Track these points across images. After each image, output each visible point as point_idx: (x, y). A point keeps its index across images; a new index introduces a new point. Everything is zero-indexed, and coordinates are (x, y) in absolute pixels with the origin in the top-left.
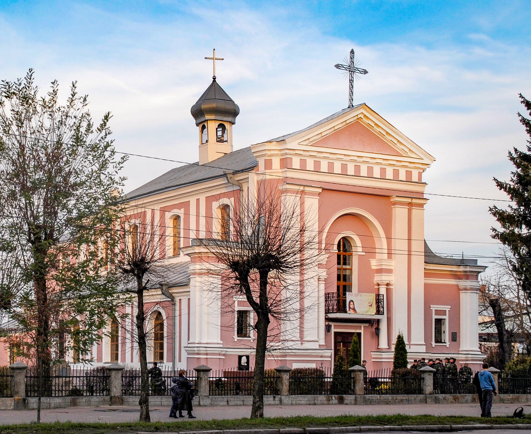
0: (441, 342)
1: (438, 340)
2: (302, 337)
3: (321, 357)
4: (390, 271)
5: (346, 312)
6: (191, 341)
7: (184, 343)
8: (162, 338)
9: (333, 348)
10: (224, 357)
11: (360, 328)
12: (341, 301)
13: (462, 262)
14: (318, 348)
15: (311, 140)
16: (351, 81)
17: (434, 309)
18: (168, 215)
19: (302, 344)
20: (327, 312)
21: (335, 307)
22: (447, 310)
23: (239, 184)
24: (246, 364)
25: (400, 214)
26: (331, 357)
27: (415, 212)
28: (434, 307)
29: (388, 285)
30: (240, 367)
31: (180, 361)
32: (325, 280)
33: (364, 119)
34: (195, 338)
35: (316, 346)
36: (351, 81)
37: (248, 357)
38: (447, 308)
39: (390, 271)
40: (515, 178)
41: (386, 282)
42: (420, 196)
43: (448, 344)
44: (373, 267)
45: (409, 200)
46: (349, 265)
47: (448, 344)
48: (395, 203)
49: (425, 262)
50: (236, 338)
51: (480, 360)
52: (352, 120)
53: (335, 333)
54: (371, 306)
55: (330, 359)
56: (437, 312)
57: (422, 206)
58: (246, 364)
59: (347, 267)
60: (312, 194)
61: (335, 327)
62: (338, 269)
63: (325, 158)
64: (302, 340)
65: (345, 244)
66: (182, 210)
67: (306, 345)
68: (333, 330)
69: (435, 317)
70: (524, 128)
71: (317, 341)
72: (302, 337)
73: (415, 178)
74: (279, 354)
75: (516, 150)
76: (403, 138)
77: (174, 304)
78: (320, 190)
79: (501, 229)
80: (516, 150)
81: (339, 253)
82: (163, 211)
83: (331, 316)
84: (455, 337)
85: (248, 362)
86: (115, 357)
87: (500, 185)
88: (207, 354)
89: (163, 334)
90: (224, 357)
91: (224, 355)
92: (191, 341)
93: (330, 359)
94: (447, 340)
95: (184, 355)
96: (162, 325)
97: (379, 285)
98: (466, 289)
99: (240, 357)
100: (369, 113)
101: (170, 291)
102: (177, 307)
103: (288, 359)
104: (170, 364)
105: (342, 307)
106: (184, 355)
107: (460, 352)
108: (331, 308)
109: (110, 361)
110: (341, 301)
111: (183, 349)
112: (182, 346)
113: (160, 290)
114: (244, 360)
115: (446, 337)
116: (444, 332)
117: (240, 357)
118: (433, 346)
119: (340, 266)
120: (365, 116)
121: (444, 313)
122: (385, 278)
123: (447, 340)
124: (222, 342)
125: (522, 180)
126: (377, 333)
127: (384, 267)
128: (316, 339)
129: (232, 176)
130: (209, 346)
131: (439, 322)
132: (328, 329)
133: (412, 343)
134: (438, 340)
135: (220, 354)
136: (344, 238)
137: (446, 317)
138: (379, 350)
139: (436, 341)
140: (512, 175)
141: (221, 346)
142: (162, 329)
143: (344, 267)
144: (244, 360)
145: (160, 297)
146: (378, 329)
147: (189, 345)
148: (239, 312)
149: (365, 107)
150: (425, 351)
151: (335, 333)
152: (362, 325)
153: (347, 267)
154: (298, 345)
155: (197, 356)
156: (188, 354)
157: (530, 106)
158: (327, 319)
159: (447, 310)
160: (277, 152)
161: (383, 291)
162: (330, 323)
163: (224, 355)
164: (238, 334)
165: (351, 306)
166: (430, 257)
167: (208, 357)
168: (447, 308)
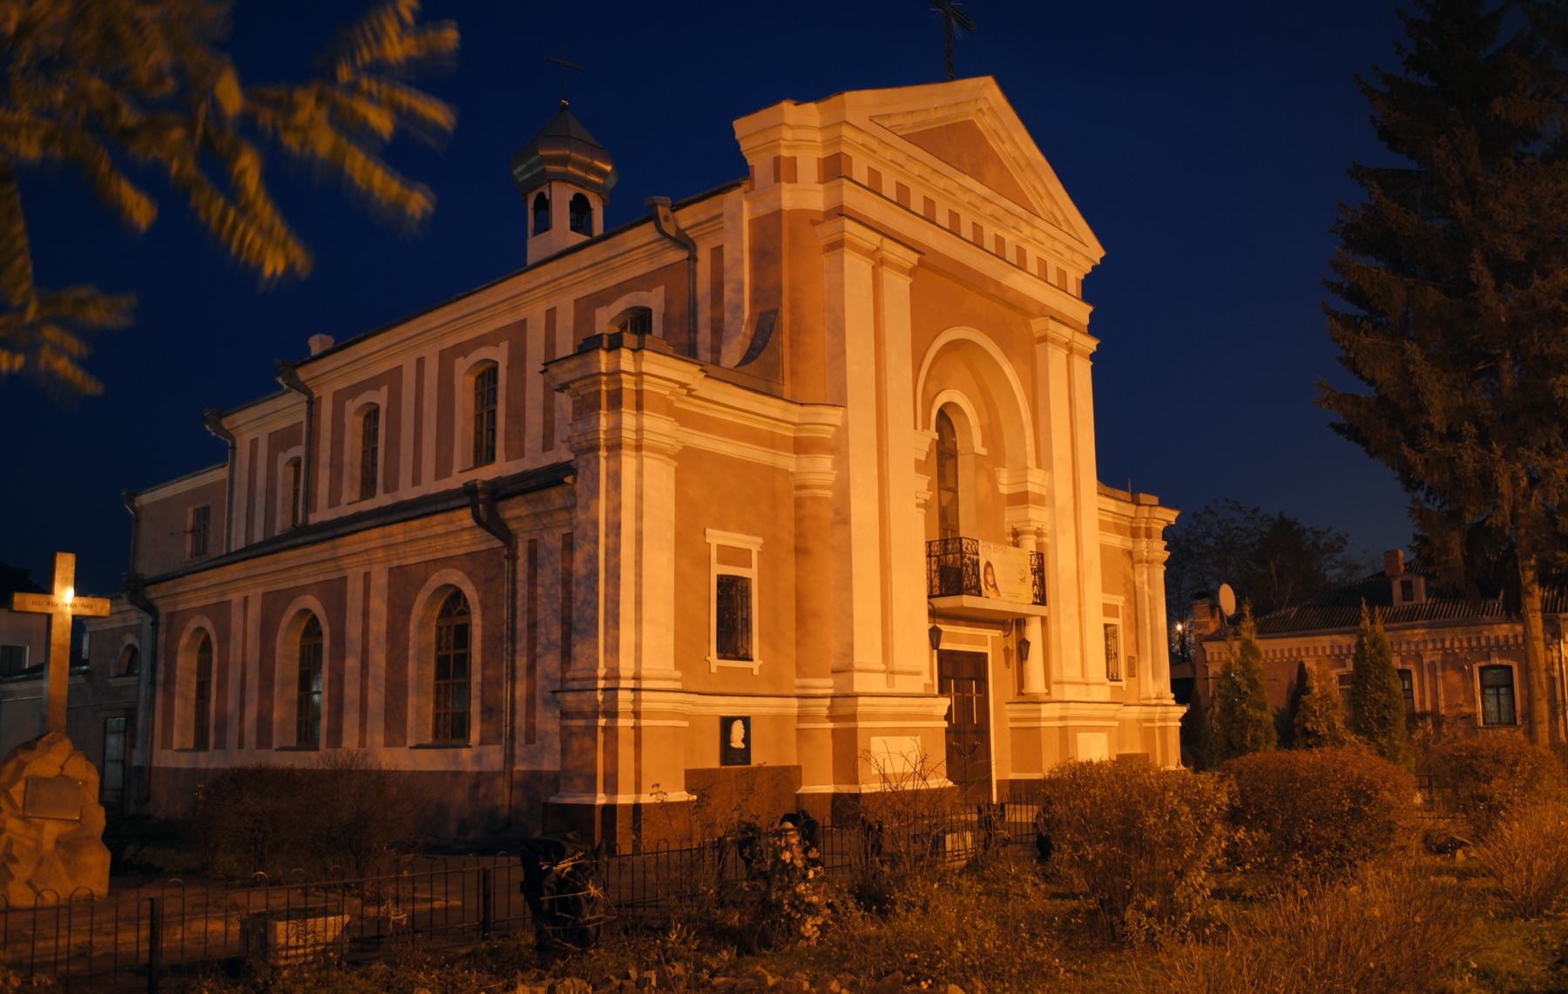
5: (979, 594)
10: (686, 724)
11: (981, 640)
14: (921, 691)
19: (889, 683)
30: (729, 754)
37: (746, 721)
54: (1023, 580)
60: (898, 268)
67: (904, 684)
71: (917, 674)
77: (513, 558)
85: (747, 740)
90: (686, 724)
99: (727, 723)
117: (727, 723)
124: (678, 674)
132: (935, 636)
141: (678, 686)
144: (738, 730)
145: (466, 536)
146: (1023, 646)
150: (1108, 699)
158: (934, 614)
159: (1120, 604)
163: (684, 716)
165: (990, 578)
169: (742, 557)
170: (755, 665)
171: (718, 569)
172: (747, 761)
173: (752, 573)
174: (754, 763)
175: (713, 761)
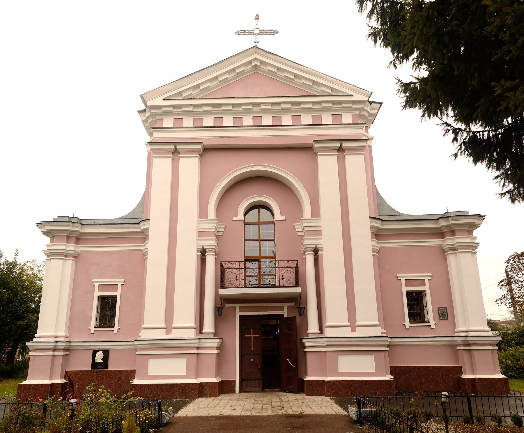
3: (198, 348)
11: (282, 308)
17: (403, 280)
24: (102, 361)
30: (95, 365)
37: (106, 353)
43: (432, 324)
49: (370, 217)
51: (491, 345)
58: (102, 361)
61: (241, 309)
84: (444, 314)
85: (106, 358)
107: (456, 334)
115: (430, 313)
118: (407, 327)
120: (262, 62)
137: (426, 288)
149: (257, 50)
152: (285, 305)
168: (426, 276)
169: (114, 287)
170: (115, 329)
171: (97, 293)
172: (107, 368)
173: (117, 293)
174: (110, 368)
175: (89, 368)
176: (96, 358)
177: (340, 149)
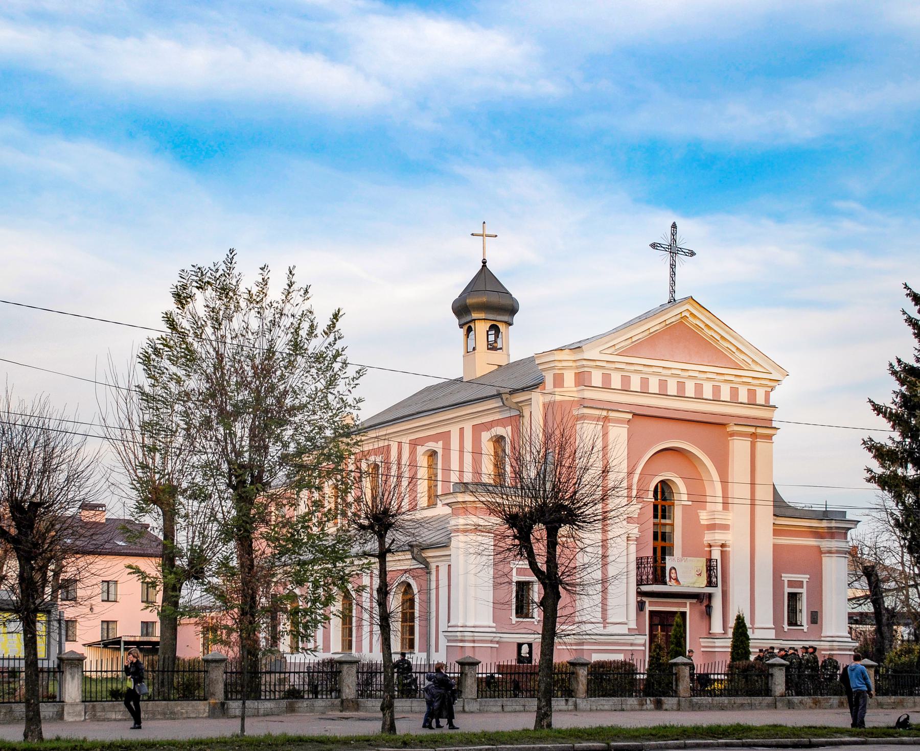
0: (796, 625)
1: (793, 622)
2: (604, 618)
3: (632, 645)
4: (725, 527)
5: (665, 583)
6: (451, 623)
7: (443, 626)
8: (412, 619)
9: (647, 632)
11: (685, 605)
12: (659, 568)
13: (825, 515)
15: (617, 347)
16: (673, 266)
18: (421, 450)
19: (604, 627)
20: (640, 583)
21: (651, 577)
22: (805, 581)
23: (519, 407)
25: (739, 448)
26: (644, 645)
27: (761, 445)
28: (786, 577)
29: (723, 546)
30: (520, 659)
31: (437, 650)
32: (637, 539)
33: (691, 319)
34: (458, 619)
35: (624, 630)
36: (673, 266)
37: (530, 645)
38: (804, 578)
39: (725, 527)
40: (898, 400)
41: (720, 543)
42: (767, 424)
43: (805, 628)
44: (703, 522)
45: (752, 430)
46: (670, 518)
47: (805, 628)
48: (732, 434)
49: (774, 515)
50: (514, 619)
51: (850, 650)
52: (673, 320)
53: (650, 611)
54: (700, 575)
55: (643, 648)
56: (791, 584)
57: (770, 437)
59: (668, 521)
60: (619, 421)
61: (651, 604)
62: (654, 524)
63: (636, 371)
64: (605, 621)
65: (664, 491)
66: (440, 443)
67: (611, 629)
68: (648, 608)
69: (787, 590)
70: (910, 330)
72: (604, 618)
73: (760, 399)
74: (573, 641)
75: (899, 361)
76: (743, 344)
77: (429, 573)
78: (630, 416)
79: (879, 470)
80: (899, 361)
81: (657, 503)
82: (414, 444)
83: (645, 588)
84: (815, 618)
85: (530, 652)
86: (348, 644)
87: (878, 409)
88: (474, 641)
89: (413, 613)
91: (498, 642)
92: (451, 623)
93: (643, 648)
94: (804, 623)
95: (443, 643)
96: (412, 601)
97: (710, 546)
98: (830, 552)
99: (520, 646)
100: (697, 309)
101: (423, 555)
102: (433, 577)
103: (585, 647)
104: (424, 655)
105: (659, 577)
106: (443, 643)
108: (644, 577)
109: (340, 651)
110: (659, 568)
111: (440, 634)
112: (440, 630)
113: (409, 553)
114: (525, 649)
115: (804, 618)
116: (801, 611)
117: (520, 646)
119: (657, 521)
120: (692, 314)
121: (800, 584)
122: (719, 537)
123: (804, 623)
125: (906, 402)
126: (708, 612)
127: (717, 522)
128: (624, 620)
129: (508, 396)
130: (477, 630)
131: (793, 597)
132: (641, 606)
133: (756, 626)
134: (793, 622)
135: (491, 642)
136: (662, 482)
137: (804, 591)
138: (711, 636)
139: (790, 624)
140: (894, 396)
141: (494, 630)
142: (412, 606)
143: (663, 521)
144: (525, 649)
145: (409, 562)
146: (709, 607)
147: (450, 629)
148: (519, 584)
149: (692, 301)
151: (650, 611)
152: (688, 602)
153: (668, 521)
154: (599, 629)
155: (461, 644)
156: (449, 641)
157: (919, 299)
158: (640, 594)
159: (805, 581)
160: (570, 364)
161: (716, 554)
162: (644, 599)
163: (498, 642)
164: (517, 613)
165: (673, 576)
166: (781, 508)
167: (476, 645)
168: (804, 578)
176: (523, 651)
177: (754, 435)
